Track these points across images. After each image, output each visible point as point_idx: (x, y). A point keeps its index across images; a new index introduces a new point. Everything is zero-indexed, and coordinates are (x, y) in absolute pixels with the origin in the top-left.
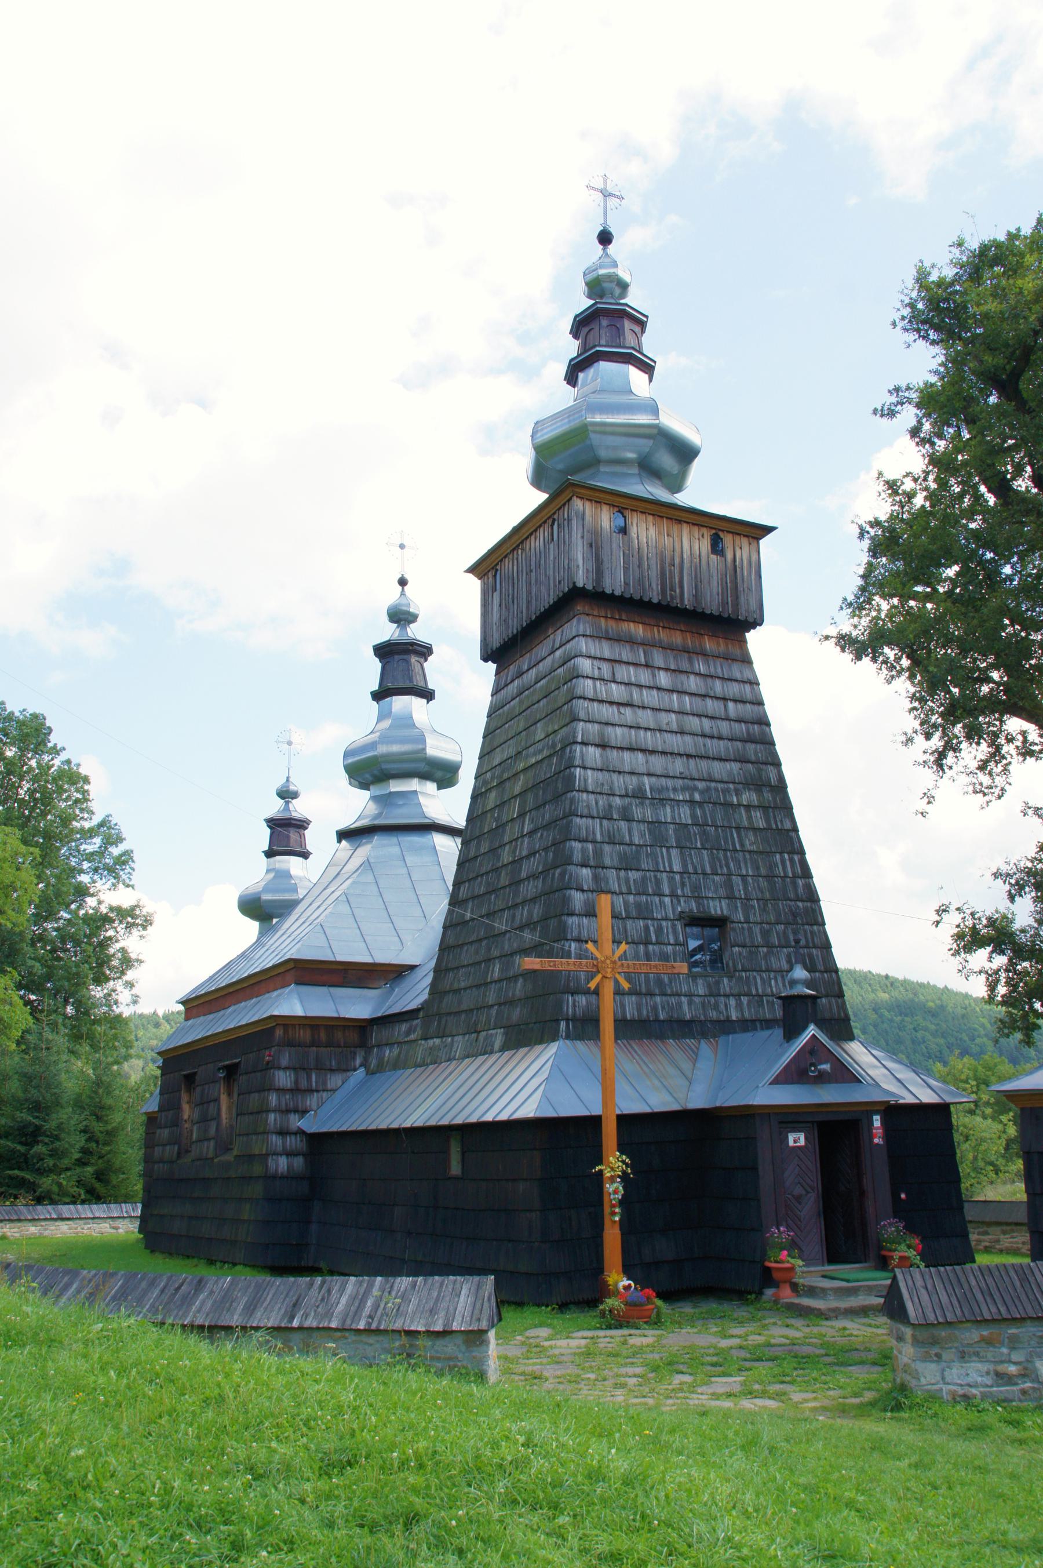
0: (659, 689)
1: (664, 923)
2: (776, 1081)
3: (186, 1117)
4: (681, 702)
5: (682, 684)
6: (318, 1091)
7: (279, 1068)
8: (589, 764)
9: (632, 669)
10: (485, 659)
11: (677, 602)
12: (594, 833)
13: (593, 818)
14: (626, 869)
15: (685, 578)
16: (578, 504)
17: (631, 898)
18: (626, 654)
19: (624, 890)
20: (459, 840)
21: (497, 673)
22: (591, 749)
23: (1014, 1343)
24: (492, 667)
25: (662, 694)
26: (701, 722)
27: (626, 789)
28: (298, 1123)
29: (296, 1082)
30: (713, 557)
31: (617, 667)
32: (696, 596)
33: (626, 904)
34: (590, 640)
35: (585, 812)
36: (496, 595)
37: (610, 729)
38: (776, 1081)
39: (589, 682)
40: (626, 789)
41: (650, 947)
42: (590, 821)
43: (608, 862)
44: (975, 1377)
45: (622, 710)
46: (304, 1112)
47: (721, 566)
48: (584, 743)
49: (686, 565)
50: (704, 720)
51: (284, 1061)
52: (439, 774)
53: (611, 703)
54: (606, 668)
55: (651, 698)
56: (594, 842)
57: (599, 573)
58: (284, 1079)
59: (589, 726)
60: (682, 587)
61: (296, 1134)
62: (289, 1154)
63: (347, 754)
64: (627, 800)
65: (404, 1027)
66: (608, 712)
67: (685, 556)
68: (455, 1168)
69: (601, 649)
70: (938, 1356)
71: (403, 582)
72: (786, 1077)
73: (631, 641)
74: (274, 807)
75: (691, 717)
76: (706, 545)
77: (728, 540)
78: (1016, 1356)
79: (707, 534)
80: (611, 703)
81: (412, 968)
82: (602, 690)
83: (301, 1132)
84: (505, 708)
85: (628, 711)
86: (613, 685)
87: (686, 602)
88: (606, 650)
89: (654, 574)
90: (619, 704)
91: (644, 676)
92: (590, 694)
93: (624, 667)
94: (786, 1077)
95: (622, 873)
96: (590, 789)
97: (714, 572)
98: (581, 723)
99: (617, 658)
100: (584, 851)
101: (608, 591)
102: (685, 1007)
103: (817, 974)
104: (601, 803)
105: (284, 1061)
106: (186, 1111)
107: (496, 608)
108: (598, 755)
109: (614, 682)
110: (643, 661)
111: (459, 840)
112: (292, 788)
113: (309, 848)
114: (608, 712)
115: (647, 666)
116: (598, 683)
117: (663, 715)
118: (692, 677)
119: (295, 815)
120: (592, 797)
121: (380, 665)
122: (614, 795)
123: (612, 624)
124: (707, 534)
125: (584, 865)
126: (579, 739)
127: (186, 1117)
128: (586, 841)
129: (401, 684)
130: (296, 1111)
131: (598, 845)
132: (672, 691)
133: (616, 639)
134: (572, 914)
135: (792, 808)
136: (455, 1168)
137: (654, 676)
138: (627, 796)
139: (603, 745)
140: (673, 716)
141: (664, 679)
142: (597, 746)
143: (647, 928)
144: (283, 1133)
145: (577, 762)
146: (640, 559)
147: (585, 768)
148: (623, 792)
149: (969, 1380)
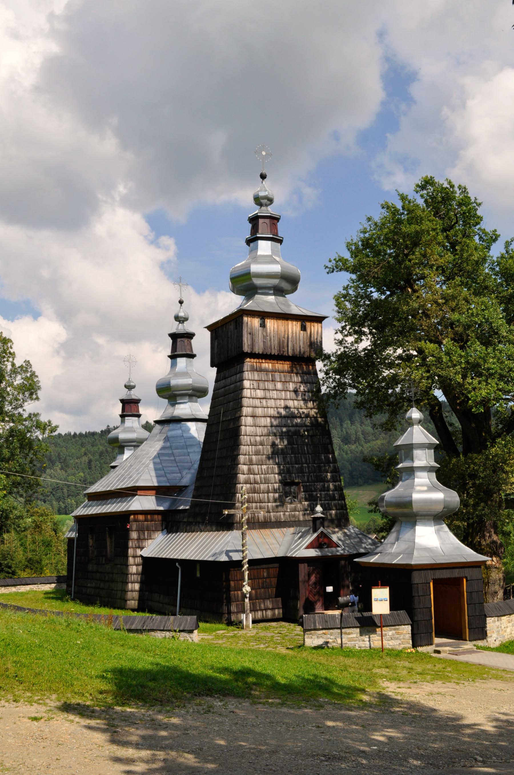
0: (276, 390)
1: (275, 485)
2: (307, 547)
3: (91, 545)
4: (286, 395)
6: (148, 539)
7: (132, 531)
8: (247, 424)
10: (212, 365)
11: (285, 354)
12: (249, 452)
13: (249, 446)
14: (261, 465)
16: (245, 319)
17: (263, 476)
18: (263, 376)
19: (260, 473)
20: (206, 424)
21: (218, 372)
22: (249, 418)
23: (331, 634)
24: (215, 369)
25: (278, 392)
26: (294, 403)
27: (262, 433)
28: (139, 552)
29: (139, 536)
30: (302, 332)
31: (260, 382)
32: (294, 350)
33: (260, 478)
34: (250, 373)
35: (246, 444)
36: (216, 341)
38: (307, 547)
39: (249, 390)
40: (262, 433)
41: (270, 494)
42: (247, 447)
43: (254, 462)
45: (262, 401)
46: (142, 548)
47: (305, 335)
48: (246, 416)
49: (290, 336)
50: (295, 401)
51: (134, 528)
52: (198, 394)
53: (257, 398)
54: (255, 383)
55: (274, 394)
56: (249, 455)
57: (253, 345)
58: (134, 535)
59: (248, 408)
60: (288, 346)
61: (139, 557)
62: (137, 565)
63: (157, 386)
64: (262, 437)
65: (182, 515)
66: (257, 402)
67: (289, 333)
68: (198, 575)
69: (254, 376)
70: (311, 637)
71: (181, 302)
72: (310, 546)
74: (124, 394)
75: (290, 401)
77: (308, 324)
78: (332, 637)
79: (299, 324)
80: (257, 398)
81: (186, 487)
82: (253, 394)
83: (141, 556)
84: (220, 390)
85: (264, 401)
89: (276, 342)
90: (260, 398)
91: (270, 386)
92: (249, 395)
94: (310, 546)
95: (259, 466)
96: (248, 434)
97: (301, 338)
98: (245, 408)
100: (245, 459)
101: (257, 352)
102: (282, 516)
103: (336, 501)
104: (252, 440)
105: (134, 528)
106: (91, 542)
107: (216, 347)
108: (251, 420)
109: (259, 389)
110: (271, 380)
111: (206, 424)
112: (132, 384)
113: (141, 412)
114: (257, 402)
115: (272, 381)
116: (252, 390)
117: (278, 401)
118: (291, 383)
119: (134, 397)
120: (248, 437)
121: (171, 341)
122: (257, 436)
124: (299, 324)
125: (244, 464)
126: (244, 415)
127: (91, 545)
128: (245, 455)
129: (181, 353)
130: (139, 547)
131: (250, 456)
133: (261, 370)
134: (240, 484)
136: (198, 575)
137: (275, 385)
138: (262, 436)
139: (253, 416)
140: (282, 401)
141: (279, 386)
142: (251, 416)
143: (268, 487)
144: (134, 557)
145: (243, 423)
147: (246, 426)
148: (261, 434)
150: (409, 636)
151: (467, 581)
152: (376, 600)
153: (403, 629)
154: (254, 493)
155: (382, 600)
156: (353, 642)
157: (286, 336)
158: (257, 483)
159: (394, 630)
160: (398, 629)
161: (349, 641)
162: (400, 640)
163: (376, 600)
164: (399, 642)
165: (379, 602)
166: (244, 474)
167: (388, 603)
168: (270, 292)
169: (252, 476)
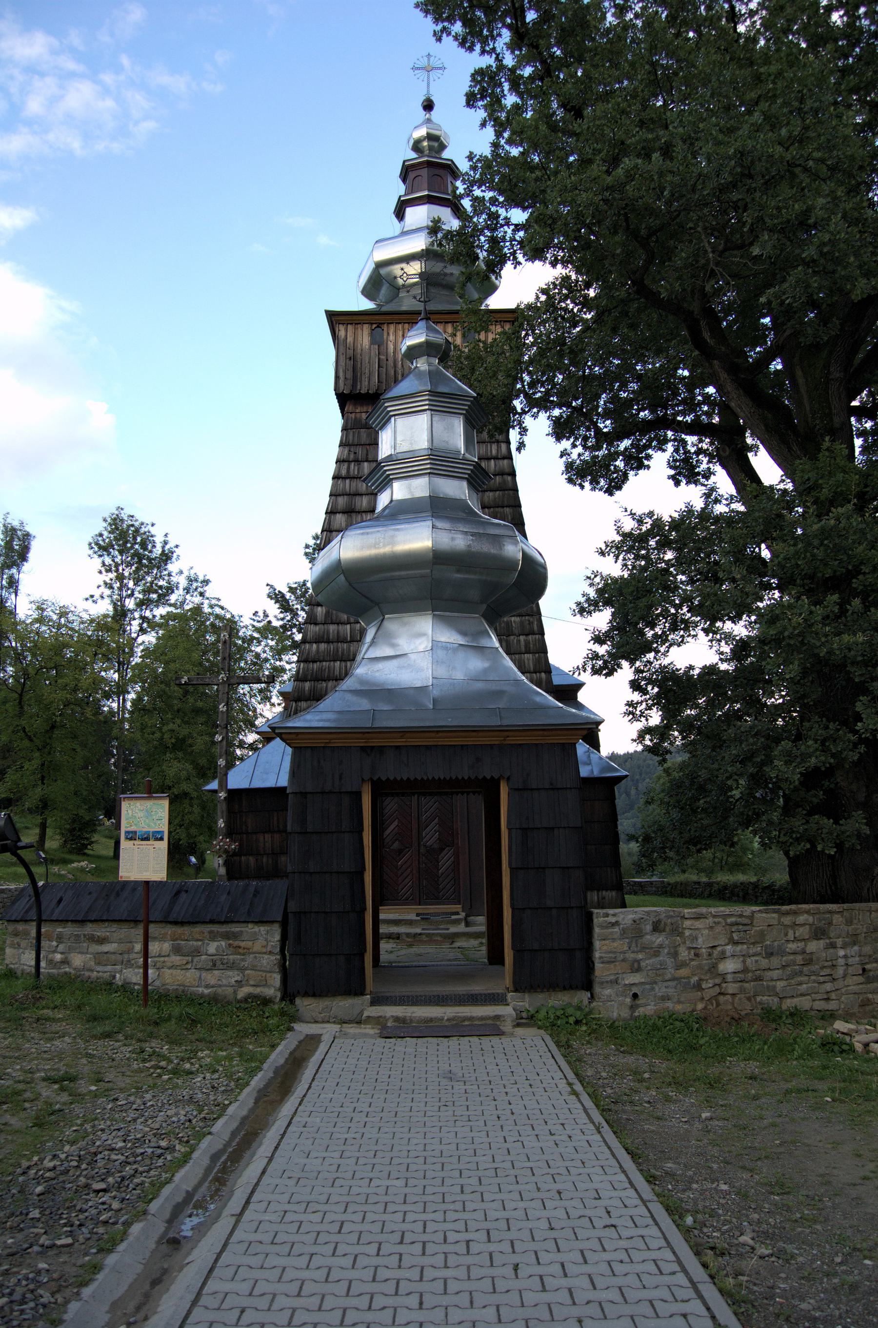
86: (366, 464)
142: (343, 512)
150: (270, 961)
151: (513, 790)
152: (132, 836)
153: (254, 938)
154: (335, 661)
155: (147, 839)
156: (109, 968)
158: (344, 641)
159: (227, 936)
160: (235, 936)
161: (99, 964)
162: (242, 970)
163: (132, 836)
164: (234, 976)
165: (137, 842)
166: (316, 624)
167: (164, 845)
169: (332, 628)
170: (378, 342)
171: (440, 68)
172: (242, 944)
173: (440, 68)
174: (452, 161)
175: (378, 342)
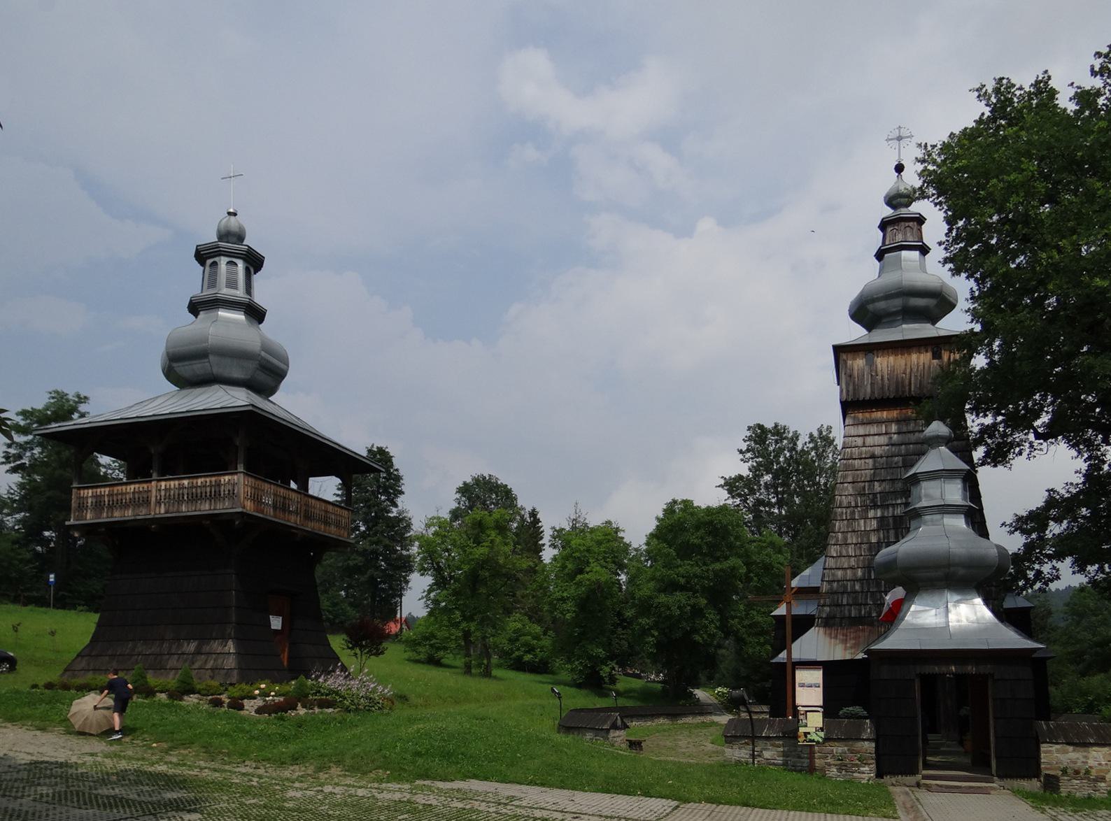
5: (909, 439)
9: (876, 437)
15: (913, 379)
37: (858, 472)
44: (742, 755)
45: (867, 461)
73: (879, 422)
76: (929, 355)
87: (913, 393)
88: (861, 430)
90: (865, 458)
93: (871, 437)
99: (867, 433)
115: (886, 434)
123: (867, 415)
132: (902, 445)
135: (981, 497)
146: (882, 376)
149: (741, 756)
157: (908, 370)
168: (899, 318)
170: (871, 364)
171: (908, 137)
172: (855, 749)
173: (908, 137)
174: (919, 214)
175: (871, 364)
